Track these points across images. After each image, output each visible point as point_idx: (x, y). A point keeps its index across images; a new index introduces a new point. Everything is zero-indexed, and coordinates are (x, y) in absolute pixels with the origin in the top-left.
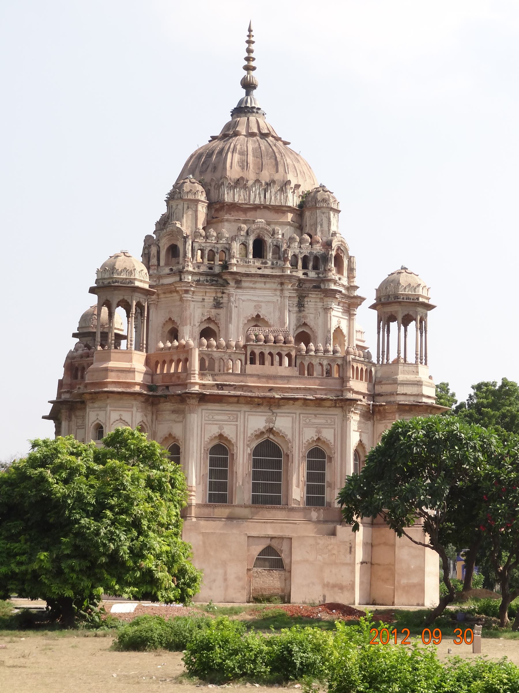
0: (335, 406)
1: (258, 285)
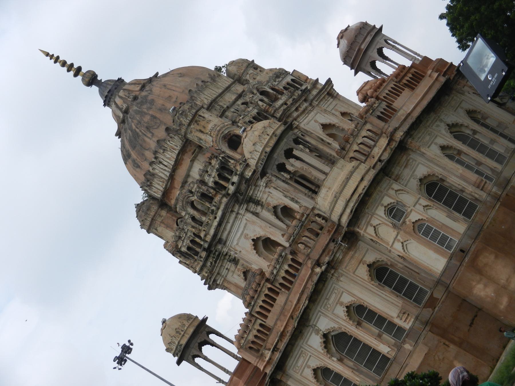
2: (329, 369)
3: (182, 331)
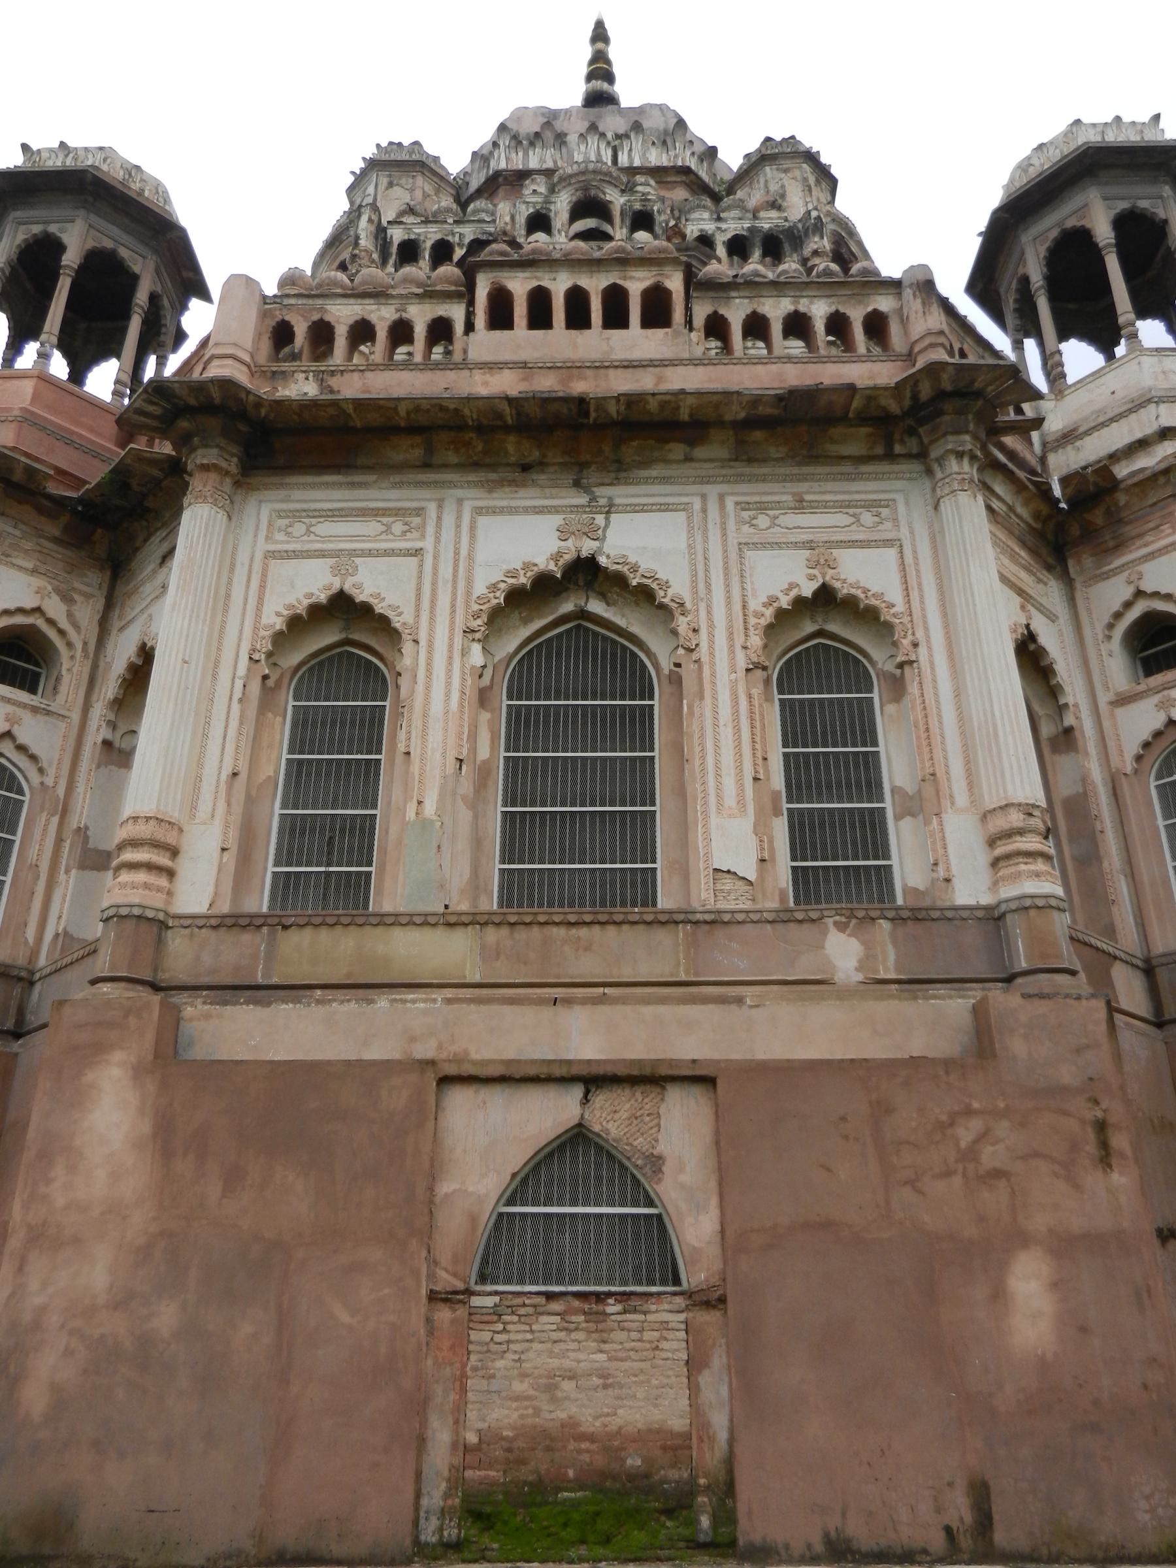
0: (890, 456)
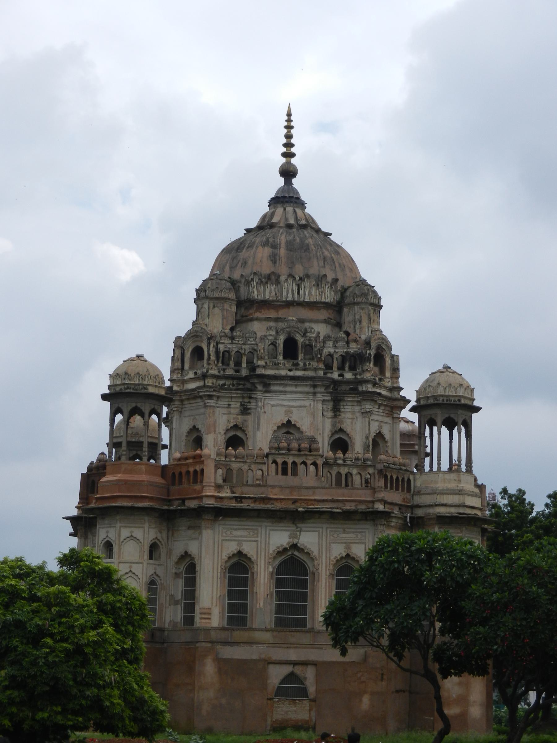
1: (288, 389)
2: (195, 568)
3: (159, 383)
